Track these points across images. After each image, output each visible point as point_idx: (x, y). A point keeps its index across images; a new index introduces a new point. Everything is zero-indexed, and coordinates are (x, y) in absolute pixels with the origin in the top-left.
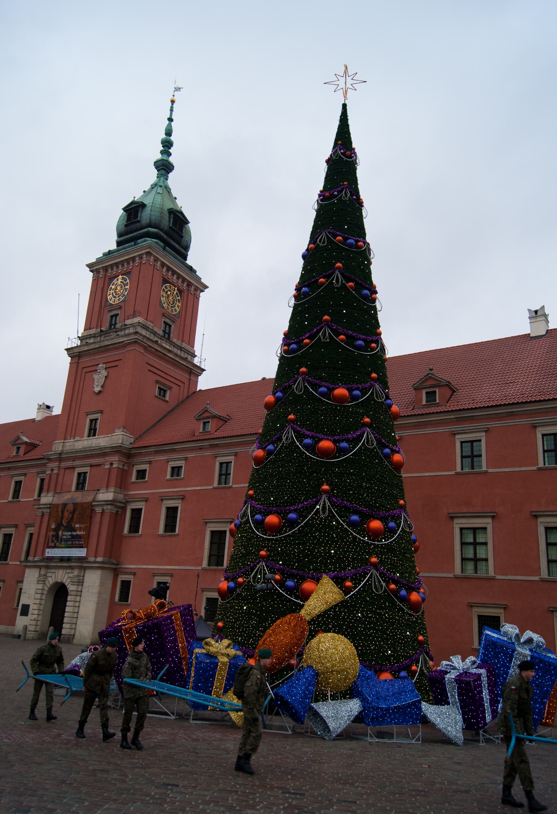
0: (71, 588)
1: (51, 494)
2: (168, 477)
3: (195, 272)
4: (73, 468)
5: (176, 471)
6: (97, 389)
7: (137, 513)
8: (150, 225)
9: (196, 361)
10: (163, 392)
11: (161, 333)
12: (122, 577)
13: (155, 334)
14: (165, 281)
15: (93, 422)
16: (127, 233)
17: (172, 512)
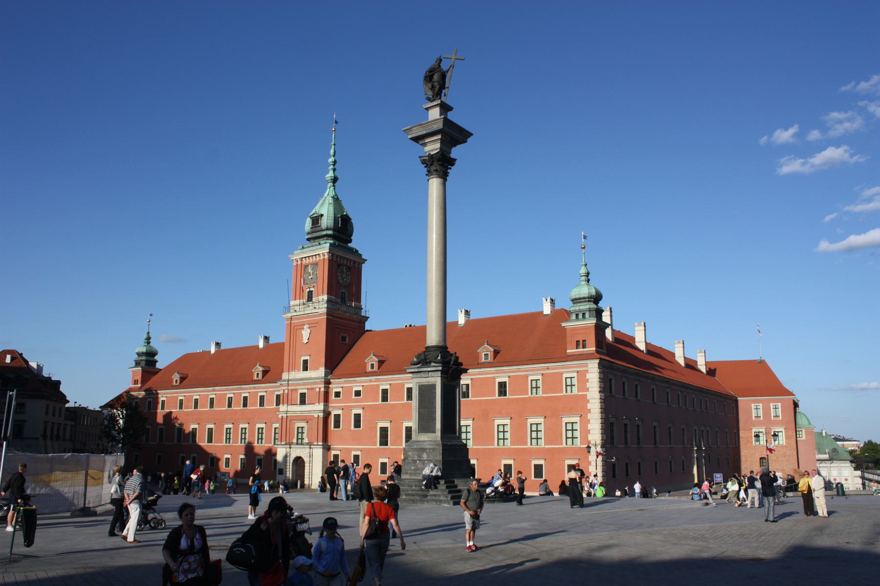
0: (306, 459)
1: (285, 405)
2: (353, 397)
3: (357, 251)
4: (296, 390)
5: (358, 393)
6: (305, 341)
7: (337, 417)
8: (327, 229)
9: (363, 314)
10: (344, 339)
11: (339, 300)
12: (333, 452)
13: (337, 303)
14: (339, 265)
15: (306, 362)
16: (313, 232)
17: (357, 417)
